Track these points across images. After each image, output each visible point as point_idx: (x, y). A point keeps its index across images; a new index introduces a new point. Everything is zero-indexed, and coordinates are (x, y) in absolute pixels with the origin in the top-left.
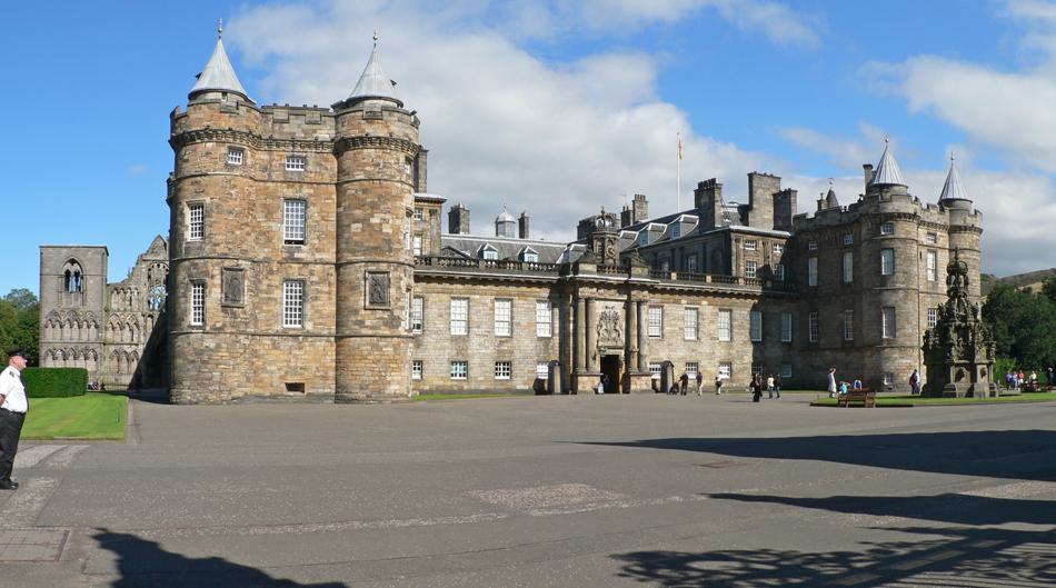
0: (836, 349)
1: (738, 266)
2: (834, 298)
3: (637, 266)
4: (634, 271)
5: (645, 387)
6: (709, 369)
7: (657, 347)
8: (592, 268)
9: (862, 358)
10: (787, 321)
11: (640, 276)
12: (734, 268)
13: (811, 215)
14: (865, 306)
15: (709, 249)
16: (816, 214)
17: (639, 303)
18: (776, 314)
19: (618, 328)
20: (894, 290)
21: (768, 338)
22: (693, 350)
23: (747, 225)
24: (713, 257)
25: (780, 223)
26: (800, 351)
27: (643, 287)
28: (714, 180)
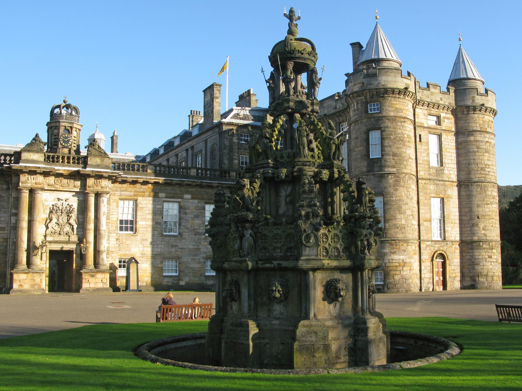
1: (231, 160)
3: (95, 156)
4: (91, 161)
5: (100, 285)
6: (192, 266)
7: (128, 242)
8: (39, 157)
11: (98, 166)
12: (226, 162)
15: (209, 145)
17: (98, 195)
19: (72, 221)
22: (173, 246)
24: (212, 152)
27: (99, 176)
28: (249, 91)
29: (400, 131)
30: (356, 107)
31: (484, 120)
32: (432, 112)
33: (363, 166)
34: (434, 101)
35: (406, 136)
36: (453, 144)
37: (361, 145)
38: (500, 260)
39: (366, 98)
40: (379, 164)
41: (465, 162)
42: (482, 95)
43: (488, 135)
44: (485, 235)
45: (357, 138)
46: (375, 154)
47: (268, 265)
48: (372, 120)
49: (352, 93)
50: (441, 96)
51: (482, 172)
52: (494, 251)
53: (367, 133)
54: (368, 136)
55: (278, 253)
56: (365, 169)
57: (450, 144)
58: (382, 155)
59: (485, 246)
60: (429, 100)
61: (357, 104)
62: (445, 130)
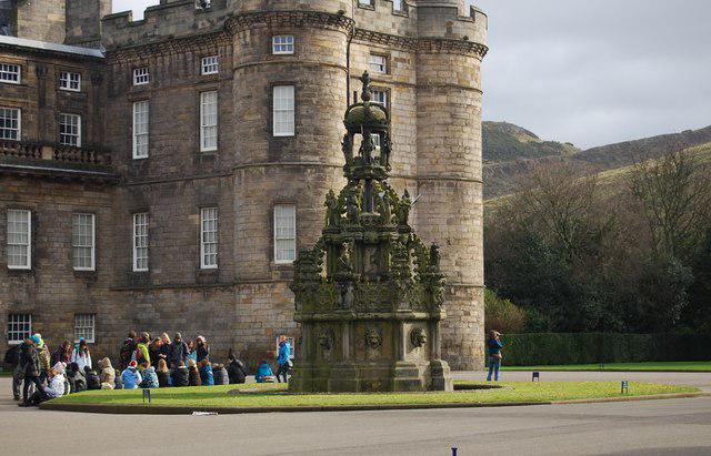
0: (183, 287)
2: (180, 184)
9: (233, 304)
10: (86, 230)
13: (138, 16)
14: (239, 203)
16: (149, 12)
18: (63, 214)
20: (299, 169)
21: (44, 262)
23: (14, 34)
25: (78, 32)
26: (112, 290)
29: (328, 89)
30: (248, 39)
31: (466, 65)
32: (377, 50)
33: (260, 149)
34: (381, 30)
35: (336, 98)
36: (410, 109)
37: (257, 111)
38: (483, 320)
39: (270, 27)
40: (290, 147)
41: (428, 142)
42: (464, 20)
43: (470, 94)
44: (460, 274)
45: (249, 97)
46: (283, 127)
47: (366, 316)
48: (280, 67)
49: (244, 14)
50: (393, 19)
51: (459, 161)
52: (474, 303)
53: (269, 90)
54: (272, 95)
55: (373, 307)
56: (263, 155)
57: (405, 108)
58: (296, 132)
59: (458, 294)
60: (372, 28)
61: (252, 34)
62: (397, 84)
